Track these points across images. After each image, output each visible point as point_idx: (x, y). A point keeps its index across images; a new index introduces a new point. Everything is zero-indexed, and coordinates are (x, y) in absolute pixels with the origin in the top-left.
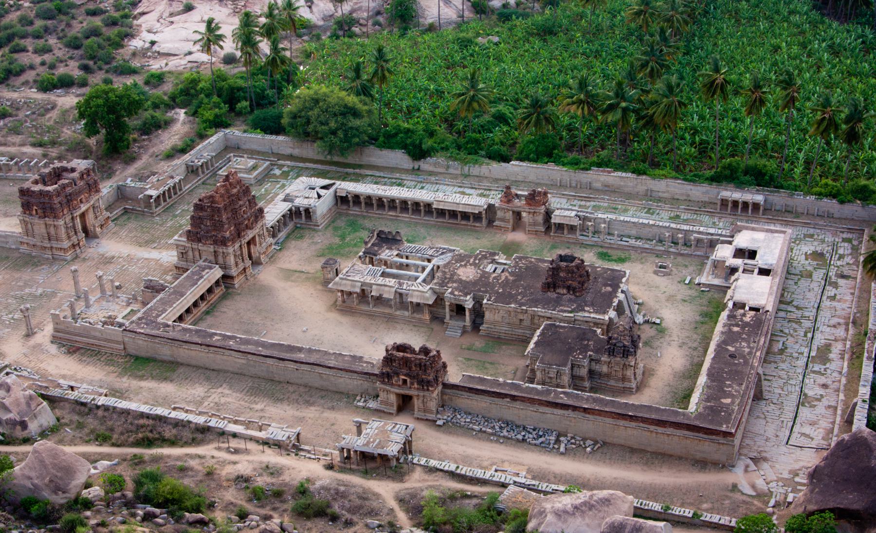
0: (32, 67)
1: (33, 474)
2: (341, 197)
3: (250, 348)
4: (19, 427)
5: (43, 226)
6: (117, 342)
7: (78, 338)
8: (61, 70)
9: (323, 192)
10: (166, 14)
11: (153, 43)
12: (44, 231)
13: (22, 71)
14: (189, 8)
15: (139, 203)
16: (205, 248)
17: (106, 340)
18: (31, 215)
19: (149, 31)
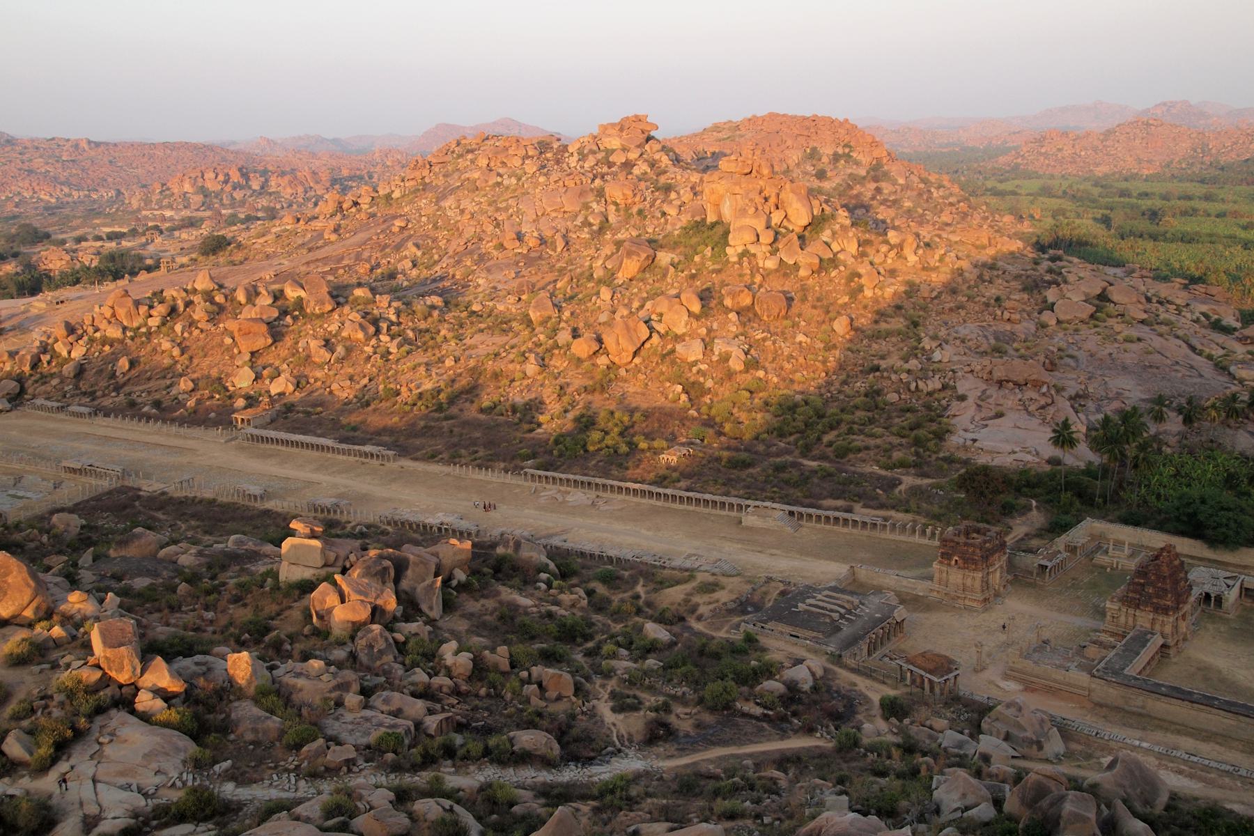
0: (867, 448)
1: (1127, 783)
2: (1247, 589)
3: (1242, 710)
4: (1035, 747)
5: (960, 576)
6: (1083, 688)
7: (1033, 679)
8: (897, 455)
9: (1230, 582)
10: (977, 418)
11: (974, 441)
12: (960, 581)
13: (859, 450)
14: (999, 415)
15: (1031, 573)
16: (1143, 614)
17: (1069, 685)
18: (949, 565)
19: (966, 430)
